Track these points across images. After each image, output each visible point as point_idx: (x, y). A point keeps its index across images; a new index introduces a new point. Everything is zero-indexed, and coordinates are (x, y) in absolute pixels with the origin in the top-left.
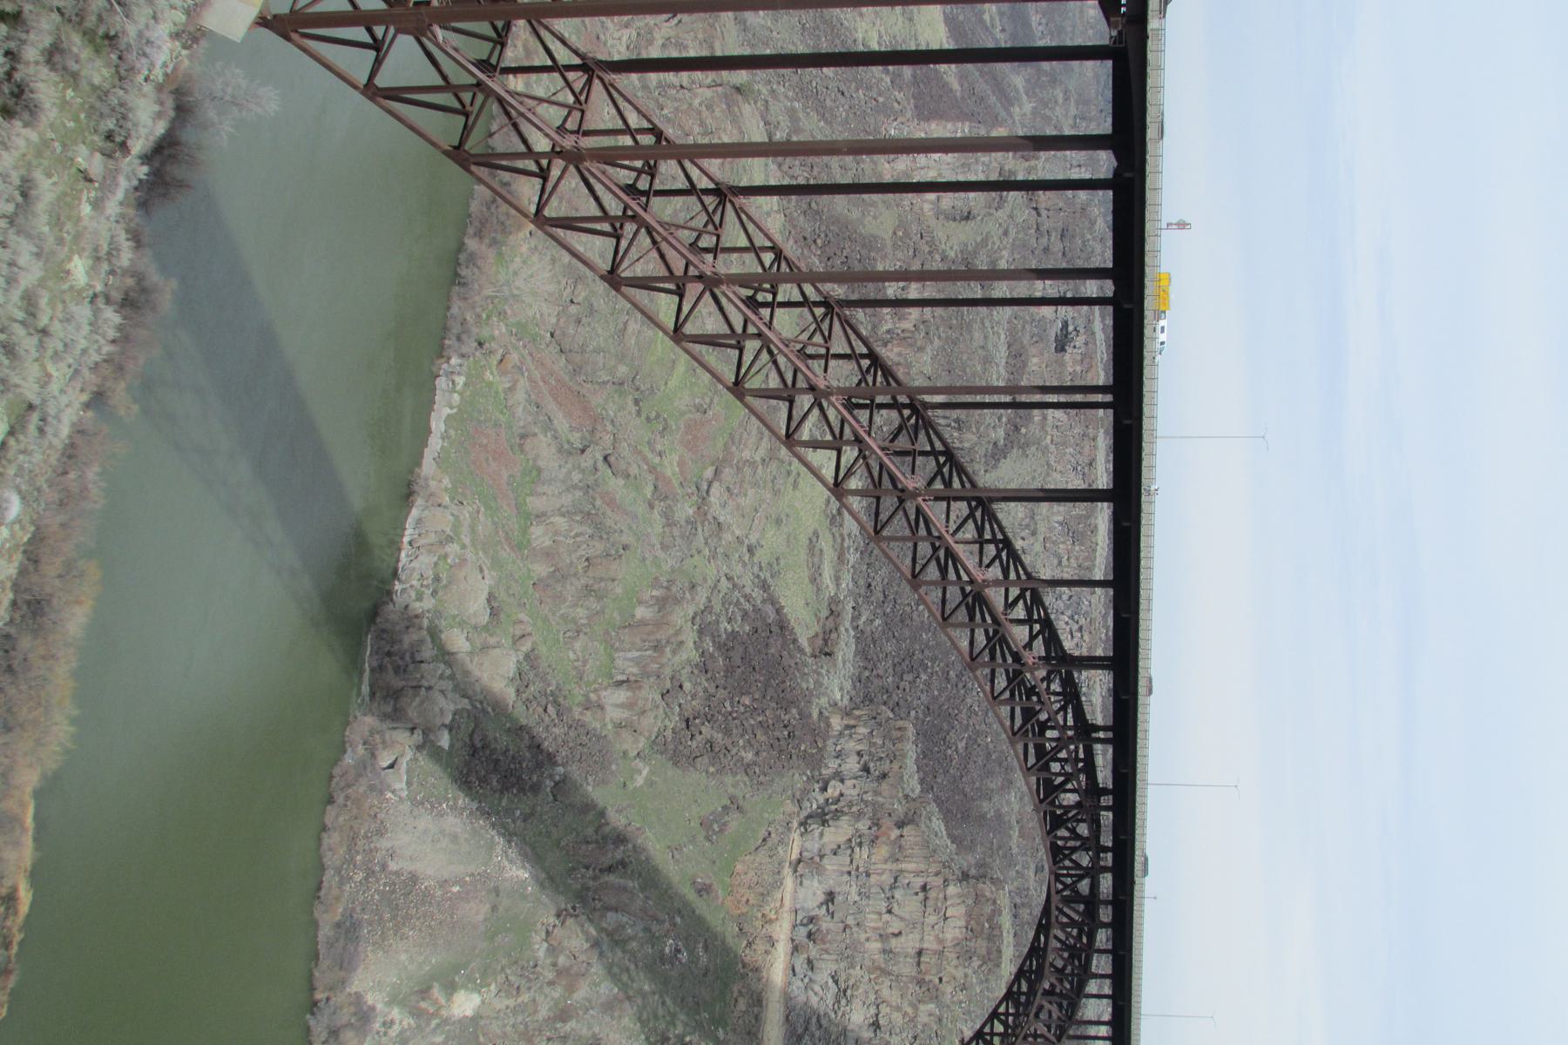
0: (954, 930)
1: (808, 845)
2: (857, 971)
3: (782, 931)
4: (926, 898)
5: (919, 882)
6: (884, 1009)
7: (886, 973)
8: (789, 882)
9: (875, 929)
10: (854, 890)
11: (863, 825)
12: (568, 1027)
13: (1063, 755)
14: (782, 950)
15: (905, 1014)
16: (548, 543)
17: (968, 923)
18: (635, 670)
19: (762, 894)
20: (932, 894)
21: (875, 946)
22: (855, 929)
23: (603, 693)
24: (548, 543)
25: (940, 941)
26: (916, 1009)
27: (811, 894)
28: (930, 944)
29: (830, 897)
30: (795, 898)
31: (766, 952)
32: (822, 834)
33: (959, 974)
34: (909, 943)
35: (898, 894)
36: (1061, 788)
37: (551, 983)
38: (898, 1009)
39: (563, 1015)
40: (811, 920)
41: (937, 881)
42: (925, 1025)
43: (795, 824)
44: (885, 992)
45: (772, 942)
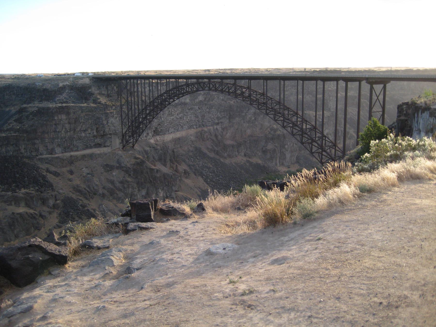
0: (64, 117)
1: (45, 153)
2: (75, 136)
3: (68, 154)
4: (58, 124)
5: (54, 126)
6: (82, 129)
7: (75, 130)
8: (57, 155)
9: (65, 134)
10: (57, 140)
11: (37, 141)
12: (122, 188)
13: (180, 91)
14: (73, 153)
15: (83, 124)
16: (24, 232)
17: (62, 114)
18: (40, 201)
19: (63, 160)
20: (57, 122)
21: (69, 134)
22: (66, 138)
23: (51, 206)
24: (24, 232)
25: (66, 119)
26: (81, 123)
27: (58, 150)
28: (67, 122)
29: (59, 145)
30: (60, 153)
31: (74, 156)
32: (42, 151)
33: (72, 114)
34: (67, 126)
35: (58, 130)
36: (222, 89)
37: (117, 194)
38: (82, 126)
39: (120, 190)
40: (65, 148)
41: (54, 122)
42: (84, 120)
43: (38, 157)
44: (78, 130)
45: (71, 156)
